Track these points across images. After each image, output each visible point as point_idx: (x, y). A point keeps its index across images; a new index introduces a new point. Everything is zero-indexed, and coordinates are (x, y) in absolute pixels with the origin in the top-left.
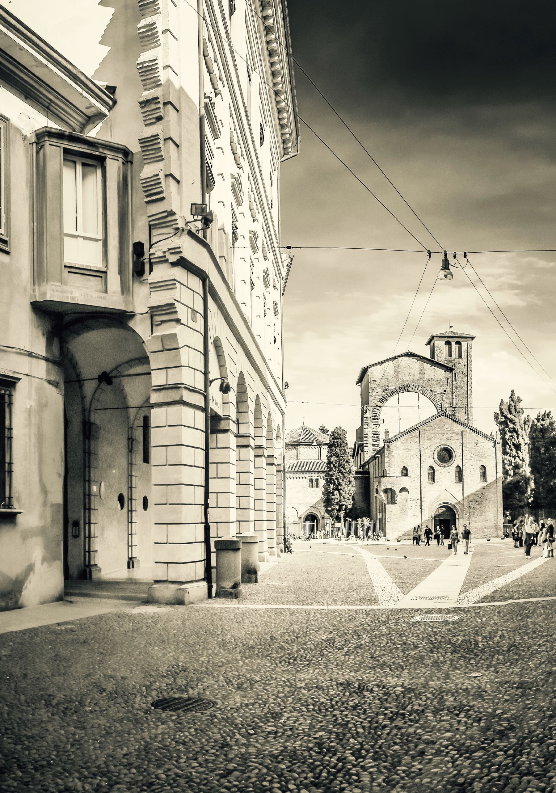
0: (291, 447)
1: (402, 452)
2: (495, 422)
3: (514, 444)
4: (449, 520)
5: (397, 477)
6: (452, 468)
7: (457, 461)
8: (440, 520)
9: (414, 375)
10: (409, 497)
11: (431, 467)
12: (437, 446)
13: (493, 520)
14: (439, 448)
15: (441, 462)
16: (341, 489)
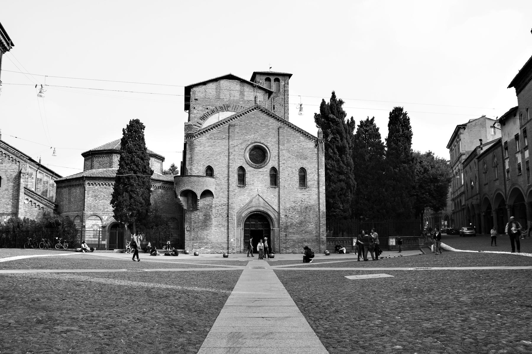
0: (105, 156)
1: (207, 149)
2: (315, 124)
3: (337, 147)
4: (262, 231)
5: (198, 176)
6: (266, 170)
7: (272, 163)
8: (251, 230)
9: (234, 96)
10: (214, 202)
11: (241, 169)
12: (249, 143)
13: (314, 233)
14: (250, 146)
15: (254, 162)
16: (132, 191)
